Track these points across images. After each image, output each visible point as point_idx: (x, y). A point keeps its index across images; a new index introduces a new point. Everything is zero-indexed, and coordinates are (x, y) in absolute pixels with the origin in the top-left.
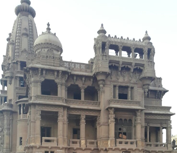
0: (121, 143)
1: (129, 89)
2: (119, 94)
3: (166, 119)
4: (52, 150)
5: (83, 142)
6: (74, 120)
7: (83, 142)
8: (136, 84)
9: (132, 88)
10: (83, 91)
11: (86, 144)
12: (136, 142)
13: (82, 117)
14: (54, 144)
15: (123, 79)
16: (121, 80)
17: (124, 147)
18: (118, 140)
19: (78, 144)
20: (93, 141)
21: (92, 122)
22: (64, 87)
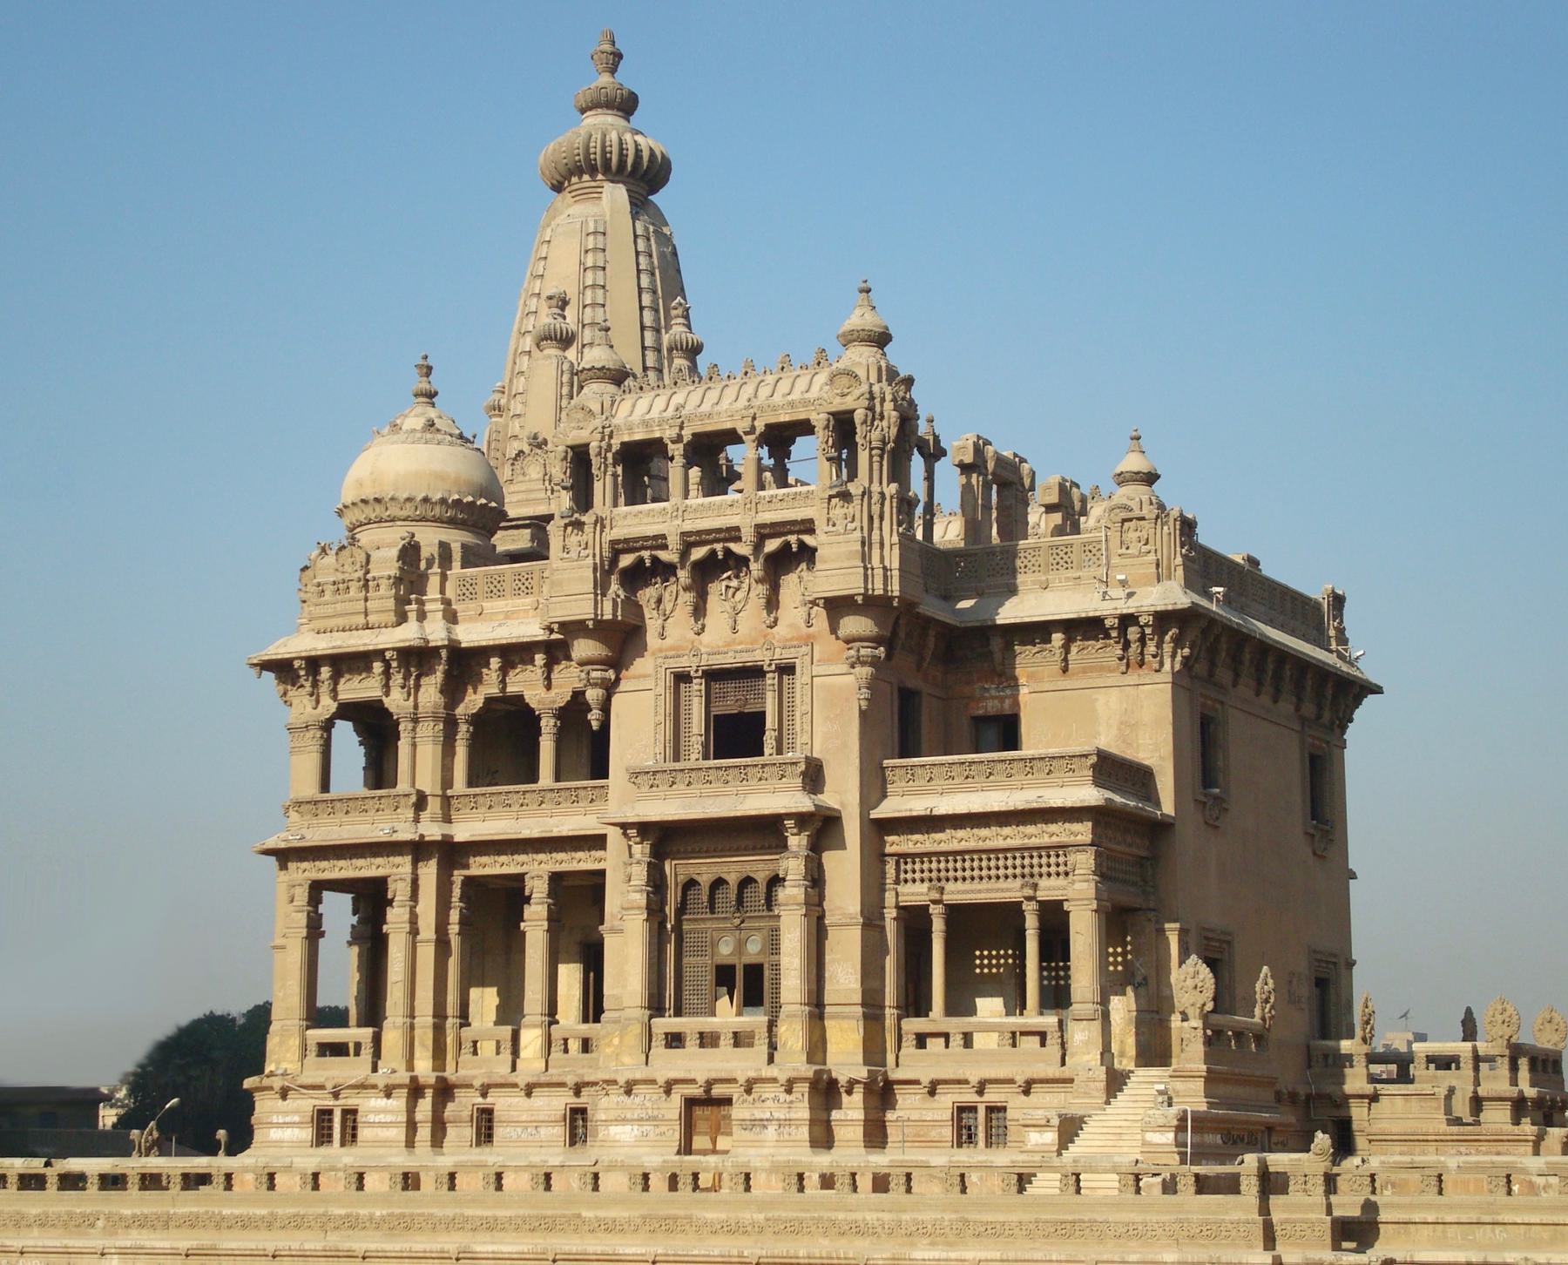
1: (771, 679)
3: (1055, 839)
4: (350, 1101)
6: (489, 916)
10: (548, 725)
13: (529, 884)
14: (352, 1069)
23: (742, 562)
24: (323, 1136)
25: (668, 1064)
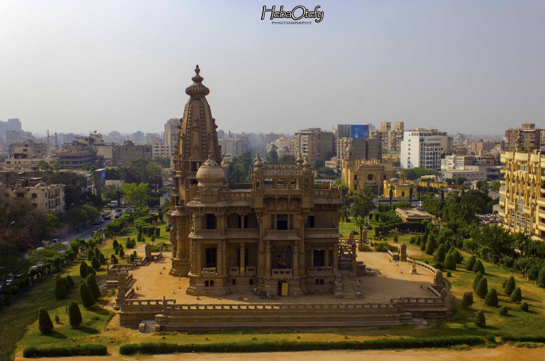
0: (276, 273)
1: (289, 217)
2: (278, 222)
5: (242, 269)
7: (242, 269)
8: (295, 211)
9: (292, 216)
11: (245, 271)
15: (280, 208)
16: (279, 208)
18: (274, 270)
19: (238, 271)
20: (252, 267)
21: (251, 248)
22: (223, 219)
23: (287, 199)
25: (275, 276)
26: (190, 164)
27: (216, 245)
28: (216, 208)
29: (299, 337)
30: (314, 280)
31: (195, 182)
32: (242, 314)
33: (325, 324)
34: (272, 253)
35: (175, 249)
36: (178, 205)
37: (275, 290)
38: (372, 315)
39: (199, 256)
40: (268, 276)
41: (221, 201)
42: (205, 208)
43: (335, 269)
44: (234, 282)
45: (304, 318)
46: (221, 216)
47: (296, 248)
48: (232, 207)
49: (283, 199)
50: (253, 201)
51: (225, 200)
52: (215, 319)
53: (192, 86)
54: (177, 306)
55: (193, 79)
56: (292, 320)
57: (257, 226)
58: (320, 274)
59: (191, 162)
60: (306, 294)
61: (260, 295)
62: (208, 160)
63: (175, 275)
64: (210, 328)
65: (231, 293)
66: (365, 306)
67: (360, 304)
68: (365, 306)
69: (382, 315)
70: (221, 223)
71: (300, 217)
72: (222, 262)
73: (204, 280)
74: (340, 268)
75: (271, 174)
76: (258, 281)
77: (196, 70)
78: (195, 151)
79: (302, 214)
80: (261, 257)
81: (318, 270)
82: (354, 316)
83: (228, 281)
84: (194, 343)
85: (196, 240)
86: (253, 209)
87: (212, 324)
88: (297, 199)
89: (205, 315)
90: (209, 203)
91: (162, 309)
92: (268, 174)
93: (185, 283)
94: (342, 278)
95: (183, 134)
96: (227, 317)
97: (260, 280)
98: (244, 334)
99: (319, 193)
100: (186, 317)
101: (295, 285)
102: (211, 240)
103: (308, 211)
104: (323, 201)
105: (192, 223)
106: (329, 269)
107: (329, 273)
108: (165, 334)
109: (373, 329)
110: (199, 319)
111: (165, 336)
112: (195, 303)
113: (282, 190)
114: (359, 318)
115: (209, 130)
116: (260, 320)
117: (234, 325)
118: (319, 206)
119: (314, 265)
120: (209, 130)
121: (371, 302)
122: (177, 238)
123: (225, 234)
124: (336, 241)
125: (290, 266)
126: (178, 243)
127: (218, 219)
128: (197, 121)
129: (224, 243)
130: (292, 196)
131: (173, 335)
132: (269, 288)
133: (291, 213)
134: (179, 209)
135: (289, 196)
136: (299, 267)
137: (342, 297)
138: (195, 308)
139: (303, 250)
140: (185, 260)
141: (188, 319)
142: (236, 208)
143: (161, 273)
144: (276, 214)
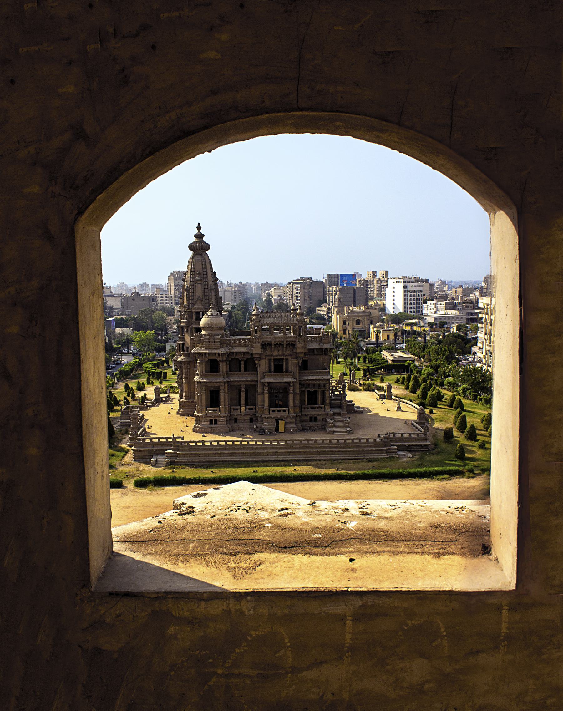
0: (274, 411)
2: (274, 365)
5: (243, 408)
7: (243, 408)
8: (291, 355)
9: (287, 360)
10: (242, 363)
12: (289, 410)
15: (276, 353)
16: (275, 353)
17: (275, 415)
18: (271, 409)
20: (252, 407)
21: (251, 389)
22: (225, 363)
23: (283, 345)
24: (211, 423)
25: (273, 415)
26: (194, 313)
27: (219, 387)
28: (219, 354)
29: (295, 470)
30: (308, 417)
31: (199, 330)
32: (243, 449)
33: (318, 457)
34: (270, 394)
35: (182, 391)
36: (183, 351)
37: (273, 427)
38: (361, 449)
39: (204, 397)
40: (266, 415)
41: (223, 347)
42: (209, 354)
43: (327, 408)
44: (236, 420)
45: (300, 452)
46: (223, 361)
47: (291, 388)
48: (233, 353)
49: (279, 344)
50: (252, 347)
51: (226, 346)
52: (219, 453)
53: (194, 242)
54: (184, 442)
55: (195, 236)
56: (289, 453)
57: (256, 369)
58: (314, 412)
59: (195, 312)
60: (301, 431)
61: (259, 432)
62: (210, 310)
63: (182, 415)
64: (215, 461)
65: (233, 430)
66: (355, 441)
67: (350, 439)
68: (355, 441)
69: (370, 449)
70: (223, 367)
71: (295, 361)
72: (224, 402)
73: (209, 419)
74: (332, 406)
75: (268, 322)
76: (257, 419)
77: (197, 228)
78: (198, 302)
79: (297, 358)
80: (259, 398)
81: (312, 408)
82: (344, 450)
83: (230, 420)
84: (201, 476)
85: (201, 382)
86: (252, 354)
87: (217, 459)
88: (292, 345)
89: (210, 450)
90: (212, 349)
91: (171, 445)
92: (265, 322)
93: (192, 422)
94: (333, 416)
95: (187, 287)
96: (230, 452)
97: (259, 418)
98: (245, 467)
99: (312, 339)
100: (194, 452)
101: (290, 423)
102: (215, 382)
103: (302, 355)
104: (315, 346)
105: (197, 367)
106: (322, 408)
107: (322, 412)
108: (174, 468)
109: (362, 461)
110: (204, 454)
111: (174, 470)
112: (201, 440)
113: (279, 336)
114: (349, 451)
115: (210, 282)
116: (260, 454)
117: (237, 459)
118: (312, 350)
119: (308, 404)
120: (210, 282)
121: (360, 437)
122: (184, 381)
123: (227, 377)
124: (327, 382)
125: (286, 405)
126: (184, 386)
127: (220, 363)
128: (199, 274)
129: (226, 385)
130: (287, 342)
131: (182, 468)
132: (267, 425)
133: (286, 357)
134: (184, 355)
135: (285, 342)
136: (295, 406)
137: (333, 433)
138: (201, 444)
139: (298, 391)
140: (190, 401)
141: (195, 454)
142: (236, 353)
143: (169, 413)
144: (272, 358)
